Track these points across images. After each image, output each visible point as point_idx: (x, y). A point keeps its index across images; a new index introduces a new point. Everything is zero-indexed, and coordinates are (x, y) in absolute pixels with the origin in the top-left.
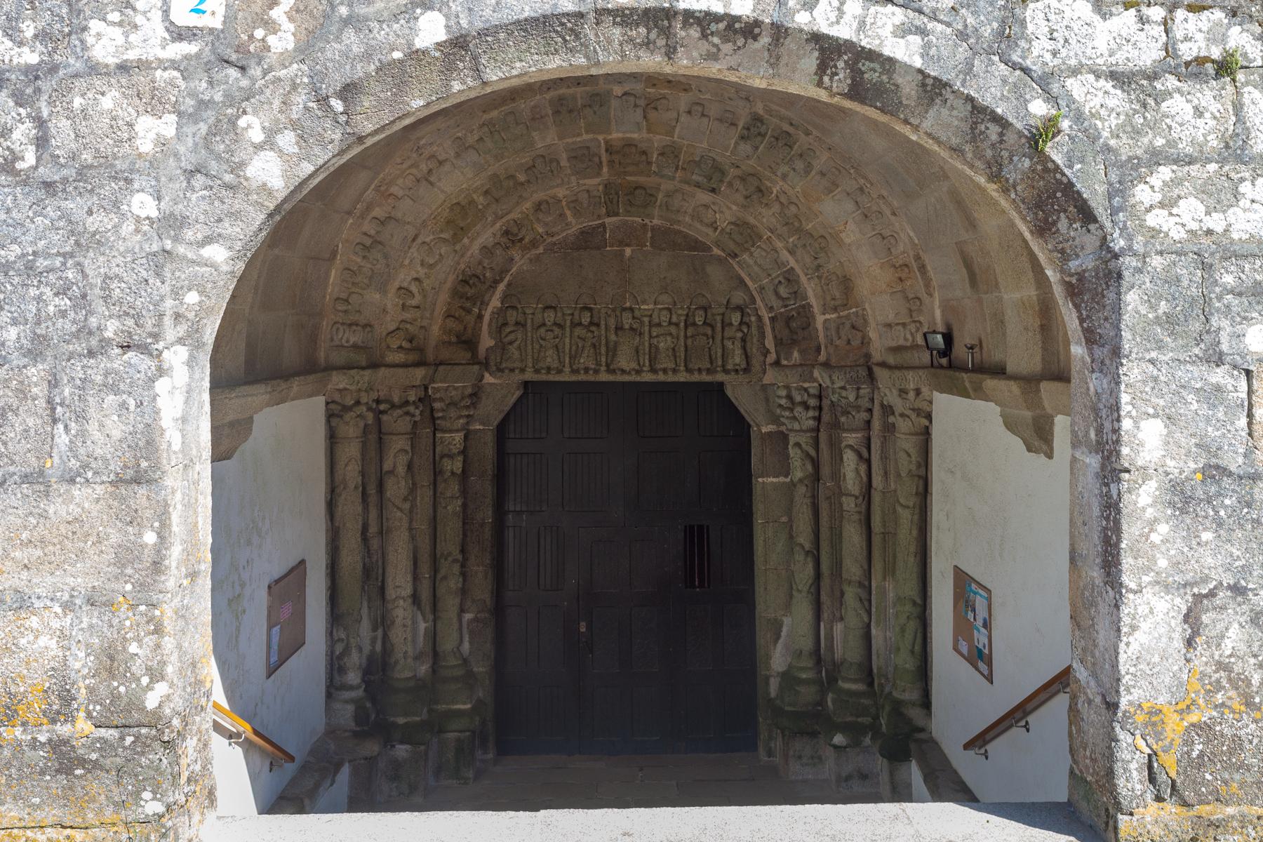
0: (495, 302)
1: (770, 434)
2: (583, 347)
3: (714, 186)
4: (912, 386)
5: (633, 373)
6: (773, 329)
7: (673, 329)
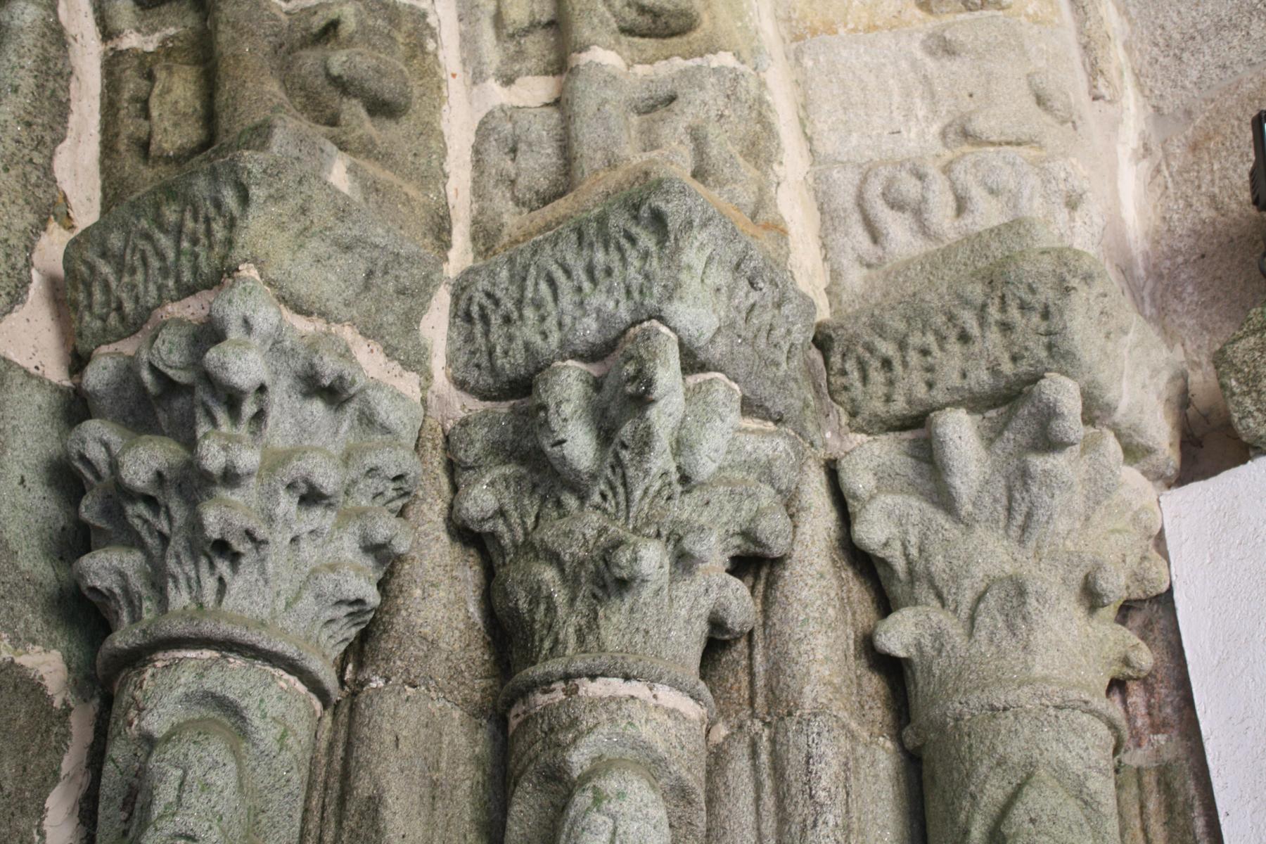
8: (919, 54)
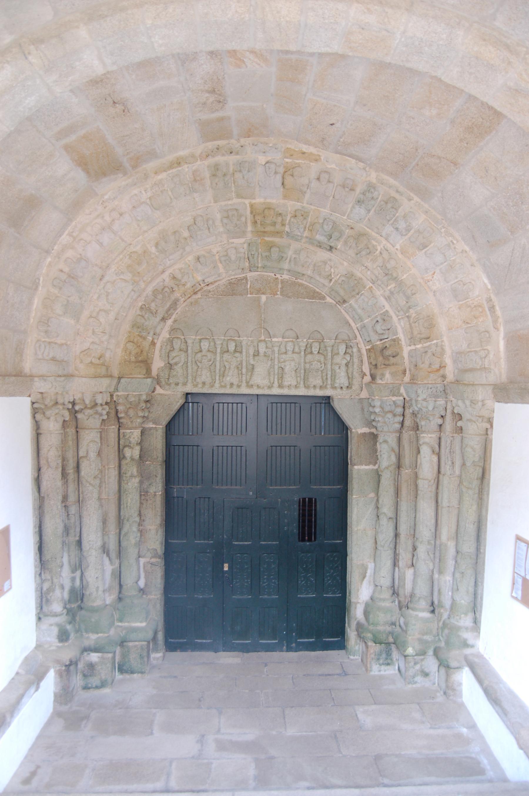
0: (165, 335)
1: (364, 434)
2: (230, 368)
3: (332, 245)
4: (480, 398)
5: (266, 388)
6: (369, 357)
7: (295, 356)
8: (464, 332)
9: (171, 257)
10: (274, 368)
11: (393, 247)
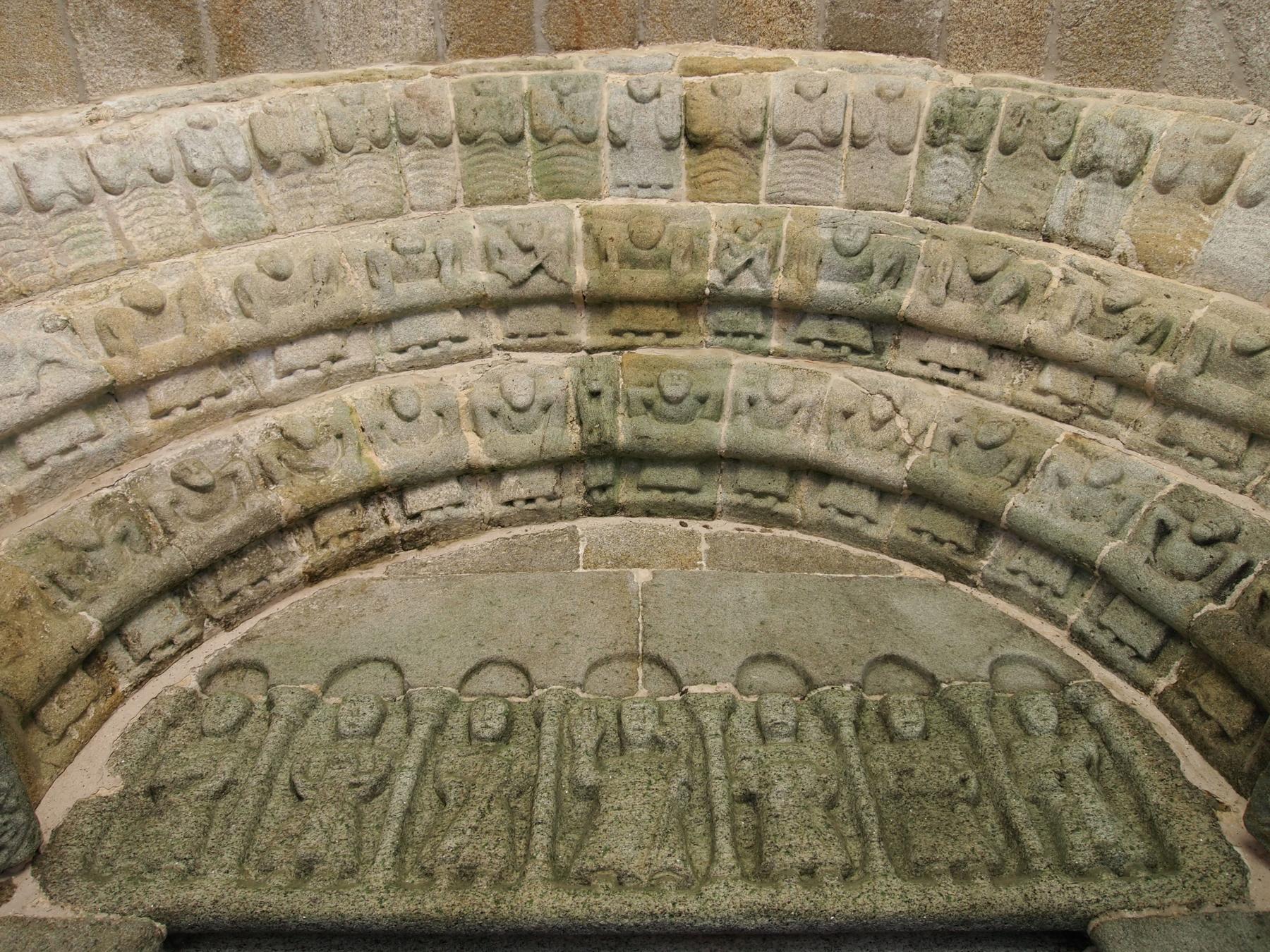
9: (287, 354)
10: (707, 801)
11: (1105, 255)
